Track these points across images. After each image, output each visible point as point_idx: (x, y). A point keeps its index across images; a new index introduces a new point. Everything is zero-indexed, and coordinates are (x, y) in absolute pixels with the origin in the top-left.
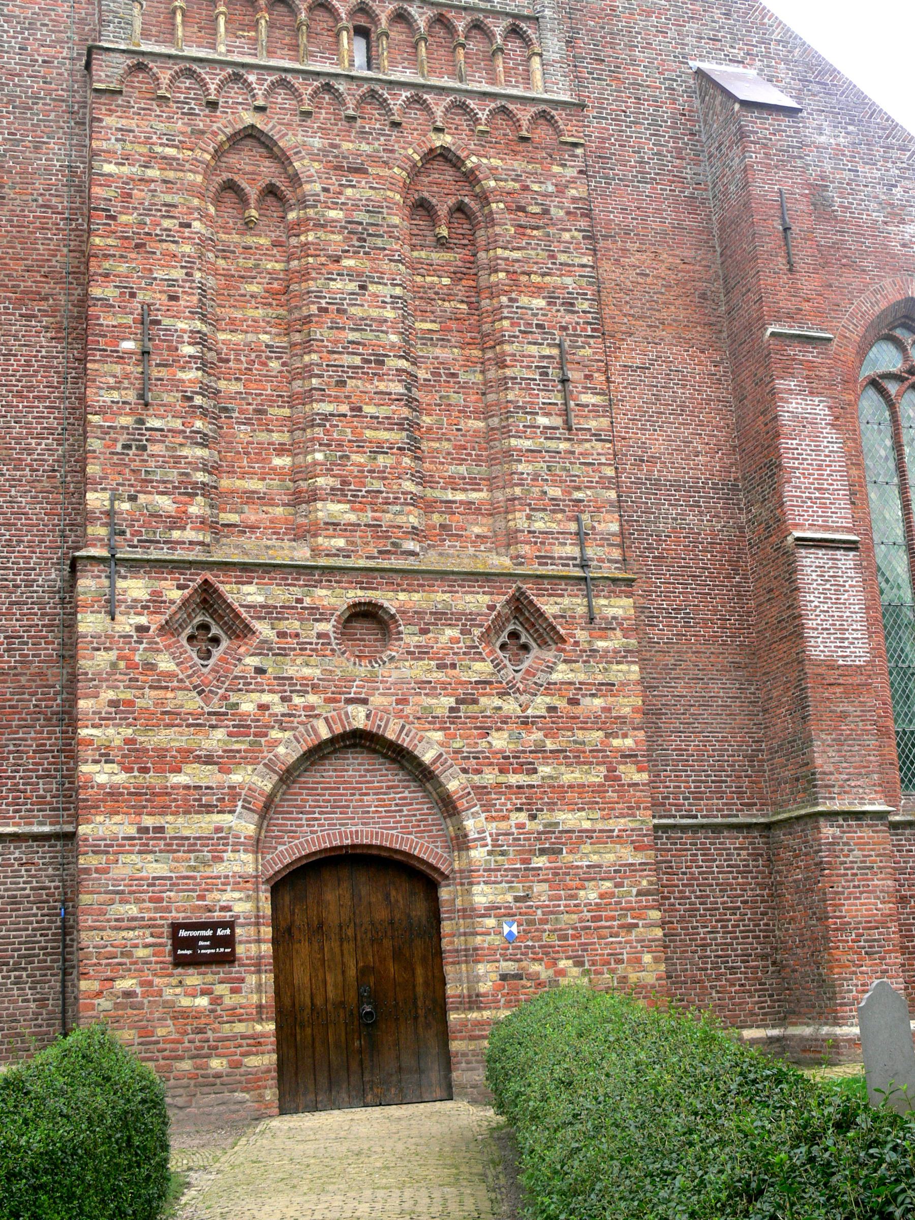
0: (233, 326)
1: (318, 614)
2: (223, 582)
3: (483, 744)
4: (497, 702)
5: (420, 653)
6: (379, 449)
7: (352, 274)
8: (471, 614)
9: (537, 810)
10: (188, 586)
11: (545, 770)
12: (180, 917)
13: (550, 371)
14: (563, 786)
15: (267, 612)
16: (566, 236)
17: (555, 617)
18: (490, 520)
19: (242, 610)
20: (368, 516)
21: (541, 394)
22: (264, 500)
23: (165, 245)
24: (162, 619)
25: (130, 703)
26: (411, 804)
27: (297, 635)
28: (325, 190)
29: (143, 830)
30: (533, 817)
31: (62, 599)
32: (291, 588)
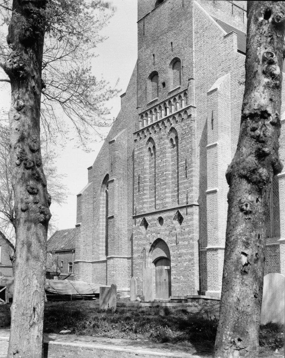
15: (150, 221)
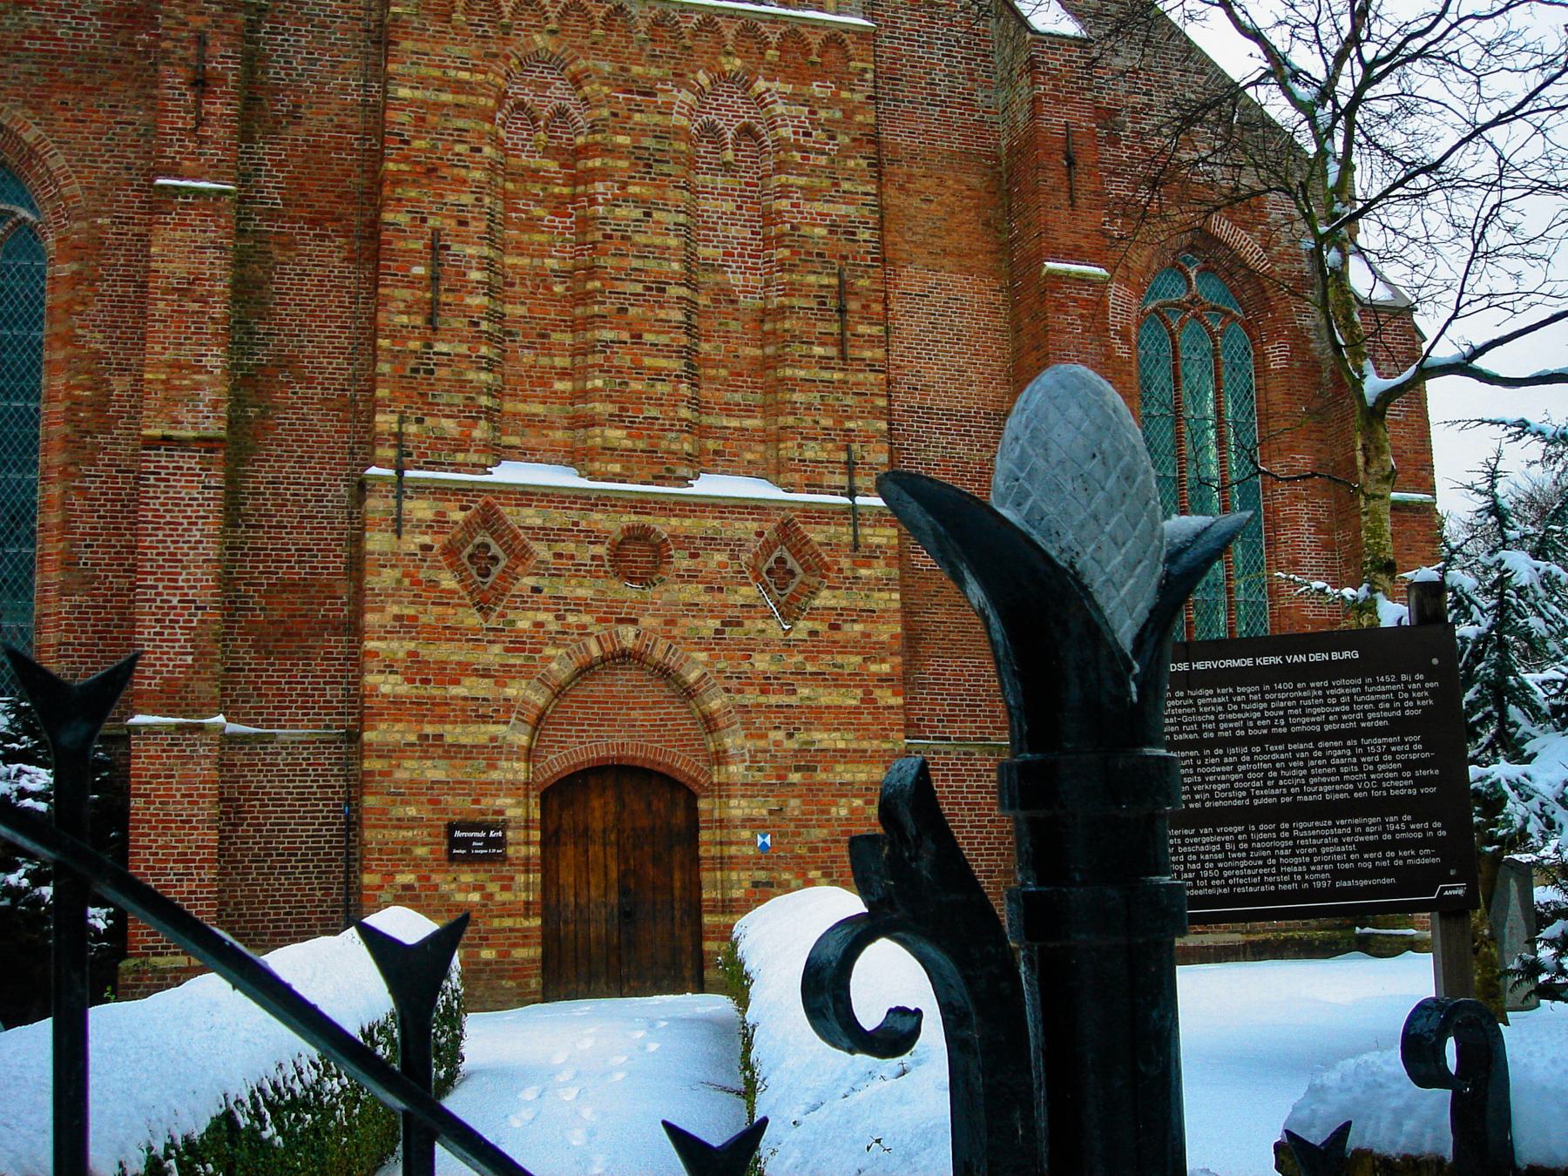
0: (520, 249)
1: (593, 537)
2: (503, 505)
3: (746, 666)
4: (760, 625)
5: (691, 576)
6: (658, 375)
7: (638, 201)
8: (739, 540)
9: (795, 729)
10: (470, 508)
11: (804, 692)
13: (828, 301)
14: (820, 707)
15: (544, 534)
16: (851, 163)
17: (821, 544)
18: (761, 448)
19: (521, 531)
21: (819, 324)
23: (456, 171)
24: (444, 539)
25: (415, 618)
26: (675, 719)
27: (572, 557)
28: (615, 115)
30: (790, 736)
31: (351, 513)
32: (568, 511)
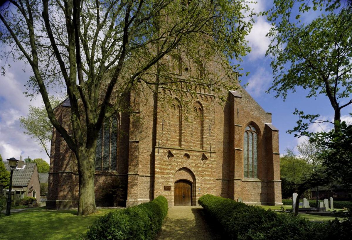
1: (181, 154)
5: (192, 159)
6: (189, 136)
11: (204, 173)
12: (165, 185)
15: (176, 154)
20: (187, 144)
22: (176, 141)
29: (161, 176)
